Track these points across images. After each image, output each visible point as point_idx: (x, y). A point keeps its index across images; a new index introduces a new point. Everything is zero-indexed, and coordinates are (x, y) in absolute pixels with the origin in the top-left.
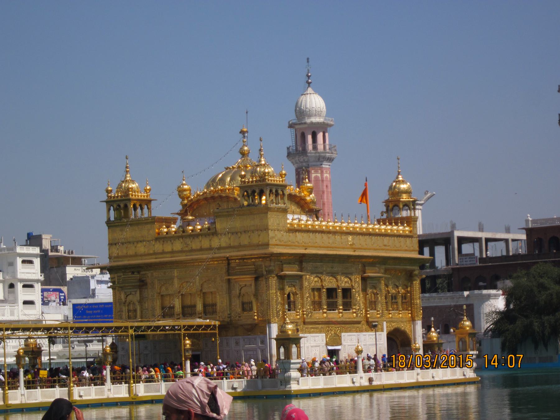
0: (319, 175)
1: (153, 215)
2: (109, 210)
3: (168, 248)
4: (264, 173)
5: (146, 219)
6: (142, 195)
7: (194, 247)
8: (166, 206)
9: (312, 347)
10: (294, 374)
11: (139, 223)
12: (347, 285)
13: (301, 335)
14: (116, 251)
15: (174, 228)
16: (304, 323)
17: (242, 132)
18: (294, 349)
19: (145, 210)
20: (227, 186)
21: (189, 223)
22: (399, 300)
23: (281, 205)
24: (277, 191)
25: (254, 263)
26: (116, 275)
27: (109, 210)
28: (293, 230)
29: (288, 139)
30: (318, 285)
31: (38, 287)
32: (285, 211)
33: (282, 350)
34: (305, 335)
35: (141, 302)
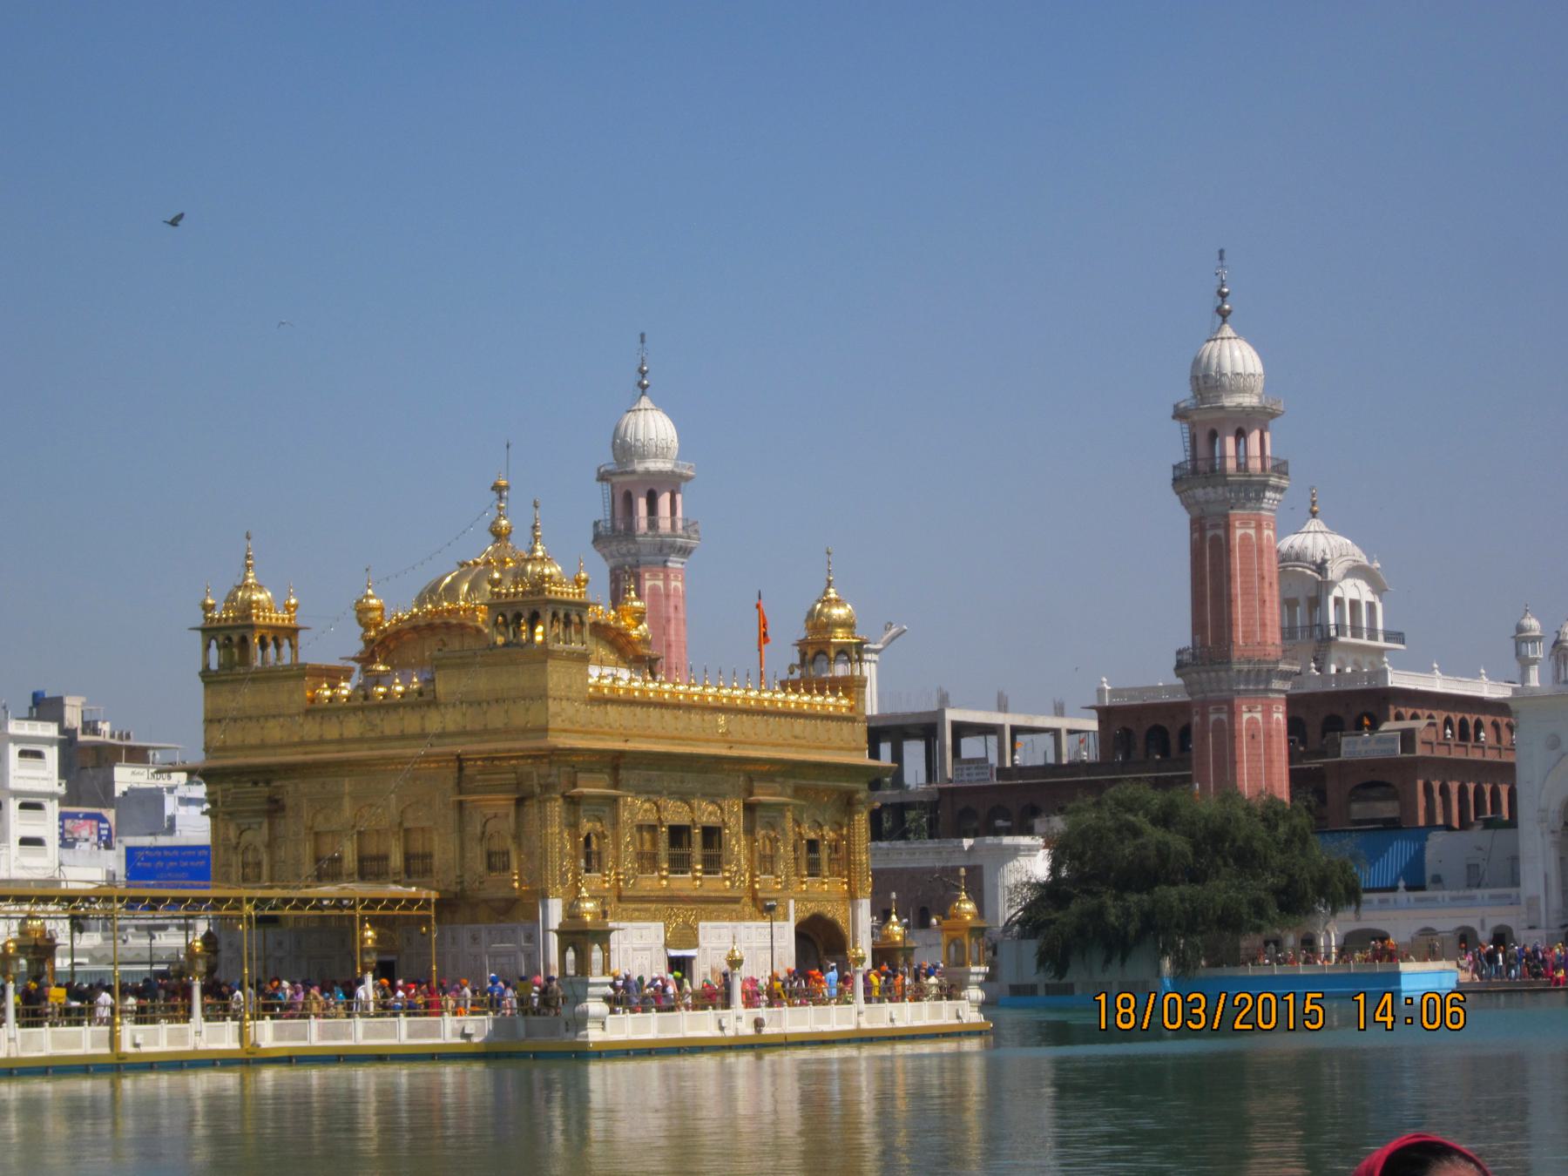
0: (660, 583)
1: (301, 660)
2: (208, 647)
3: (332, 731)
4: (542, 577)
5: (287, 668)
6: (279, 617)
7: (388, 731)
8: (331, 642)
10: (596, 1007)
11: (271, 676)
12: (713, 821)
13: (611, 925)
14: (219, 737)
15: (345, 689)
16: (620, 899)
17: (497, 488)
18: (596, 954)
21: (378, 679)
23: (575, 646)
24: (567, 616)
25: (514, 770)
26: (218, 788)
28: (601, 700)
29: (596, 505)
30: (652, 818)
31: (53, 809)
32: (584, 659)
33: (571, 955)
34: (622, 925)
35: (271, 845)
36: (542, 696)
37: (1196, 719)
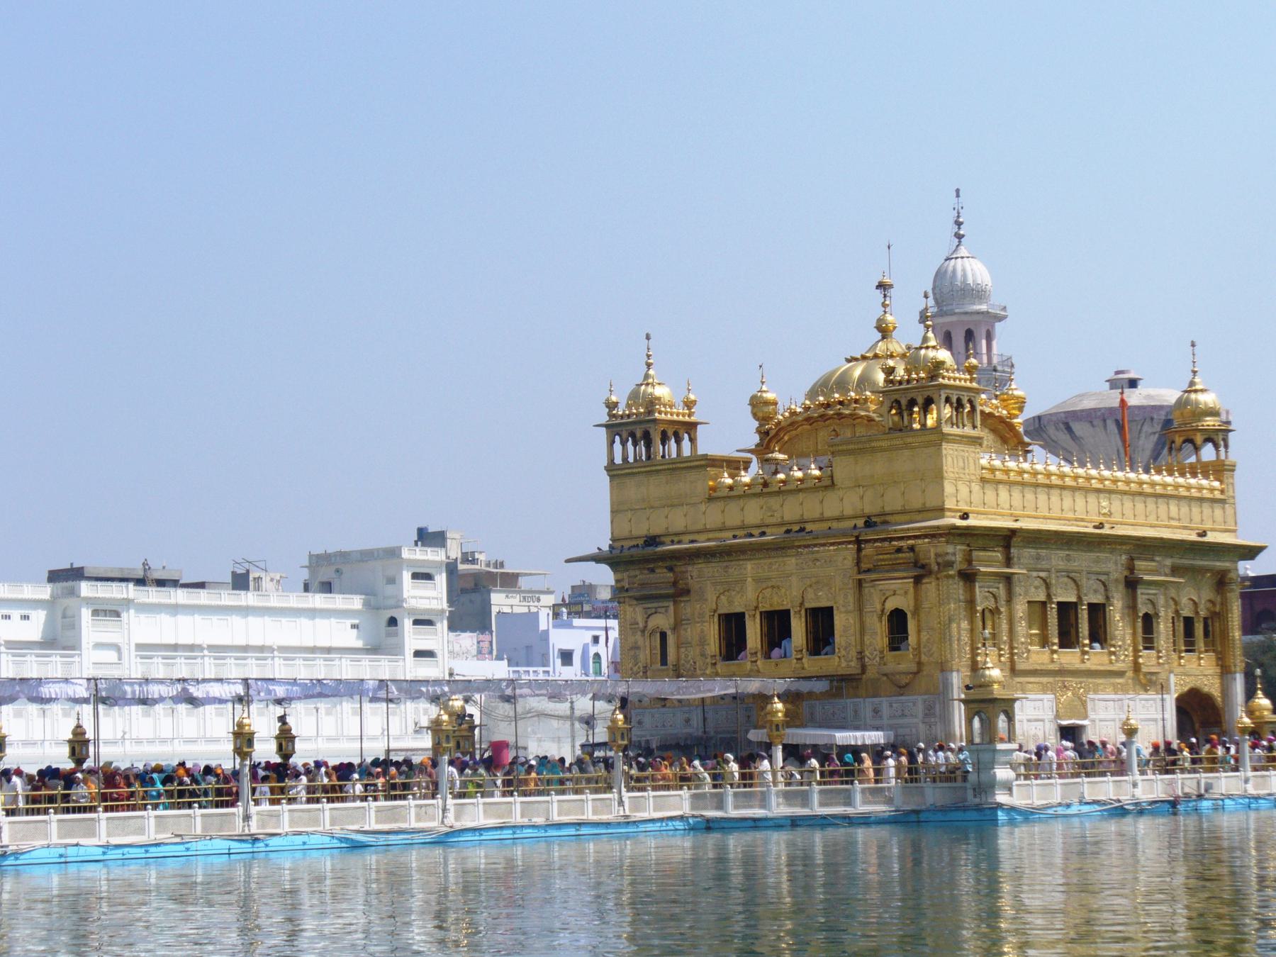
1: (700, 452)
5: (688, 460)
6: (678, 414)
9: (1029, 721)
12: (1097, 599)
15: (746, 478)
17: (882, 286)
18: (1002, 722)
19: (686, 443)
20: (852, 394)
21: (777, 467)
23: (968, 430)
24: (959, 400)
25: (912, 549)
26: (625, 575)
27: (611, 443)
30: (1042, 598)
33: (976, 723)
36: (939, 477)
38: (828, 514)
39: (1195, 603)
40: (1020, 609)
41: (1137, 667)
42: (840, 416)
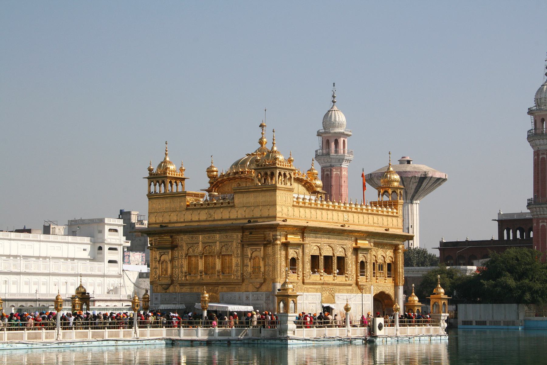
0: (339, 173)
2: (150, 185)
5: (180, 193)
6: (178, 175)
7: (216, 218)
8: (197, 184)
12: (342, 254)
16: (303, 283)
17: (261, 126)
18: (291, 305)
22: (385, 268)
24: (285, 174)
26: (153, 238)
29: (316, 144)
30: (317, 253)
33: (282, 305)
35: (172, 260)
36: (274, 205)
37: (535, 224)
38: (232, 217)
39: (384, 257)
40: (308, 259)
41: (357, 283)
42: (241, 178)
